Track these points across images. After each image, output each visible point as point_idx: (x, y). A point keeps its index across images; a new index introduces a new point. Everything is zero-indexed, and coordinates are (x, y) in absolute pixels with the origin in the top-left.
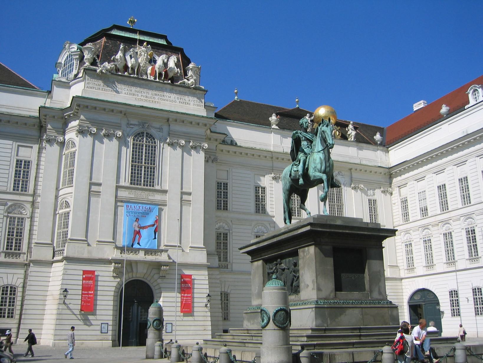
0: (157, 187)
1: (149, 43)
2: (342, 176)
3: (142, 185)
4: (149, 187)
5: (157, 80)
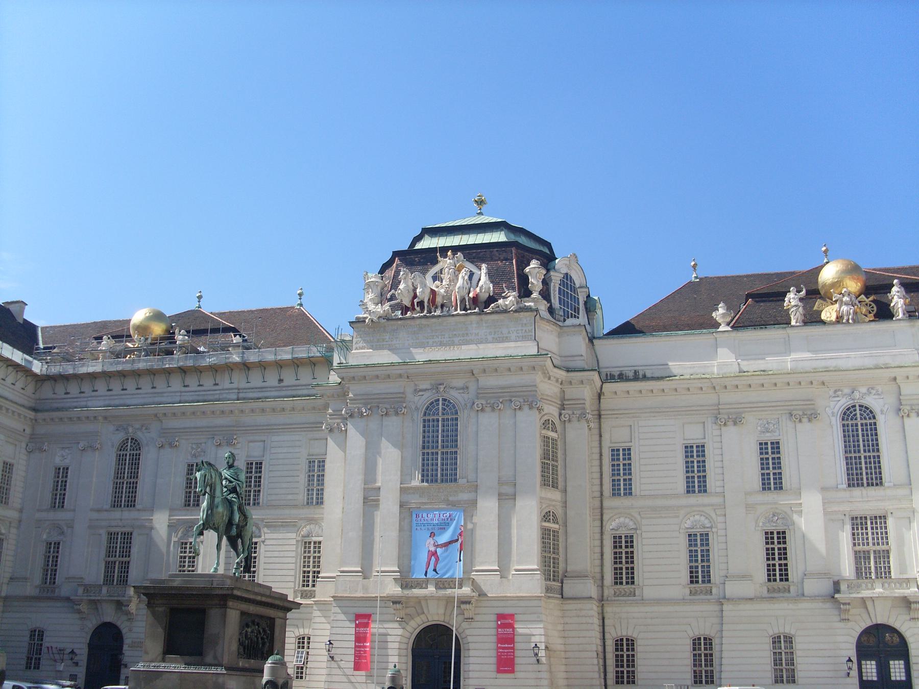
1: (455, 249)
2: (877, 397)
5: (459, 311)
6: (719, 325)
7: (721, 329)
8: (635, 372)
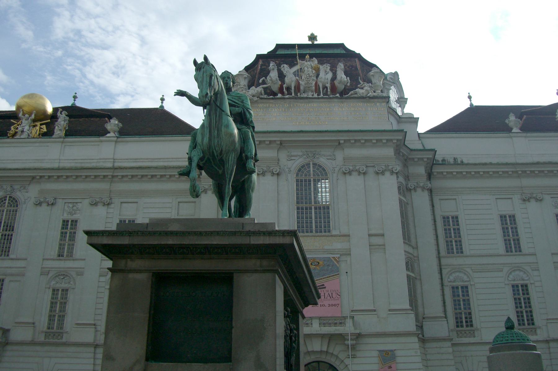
0: (334, 232)
3: (314, 231)
4: (323, 234)
6: (512, 129)
7: (513, 131)
8: (455, 159)
